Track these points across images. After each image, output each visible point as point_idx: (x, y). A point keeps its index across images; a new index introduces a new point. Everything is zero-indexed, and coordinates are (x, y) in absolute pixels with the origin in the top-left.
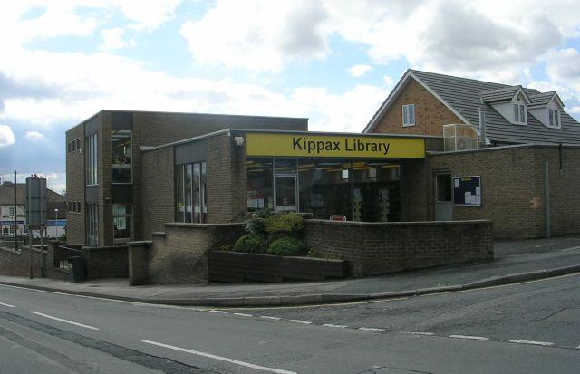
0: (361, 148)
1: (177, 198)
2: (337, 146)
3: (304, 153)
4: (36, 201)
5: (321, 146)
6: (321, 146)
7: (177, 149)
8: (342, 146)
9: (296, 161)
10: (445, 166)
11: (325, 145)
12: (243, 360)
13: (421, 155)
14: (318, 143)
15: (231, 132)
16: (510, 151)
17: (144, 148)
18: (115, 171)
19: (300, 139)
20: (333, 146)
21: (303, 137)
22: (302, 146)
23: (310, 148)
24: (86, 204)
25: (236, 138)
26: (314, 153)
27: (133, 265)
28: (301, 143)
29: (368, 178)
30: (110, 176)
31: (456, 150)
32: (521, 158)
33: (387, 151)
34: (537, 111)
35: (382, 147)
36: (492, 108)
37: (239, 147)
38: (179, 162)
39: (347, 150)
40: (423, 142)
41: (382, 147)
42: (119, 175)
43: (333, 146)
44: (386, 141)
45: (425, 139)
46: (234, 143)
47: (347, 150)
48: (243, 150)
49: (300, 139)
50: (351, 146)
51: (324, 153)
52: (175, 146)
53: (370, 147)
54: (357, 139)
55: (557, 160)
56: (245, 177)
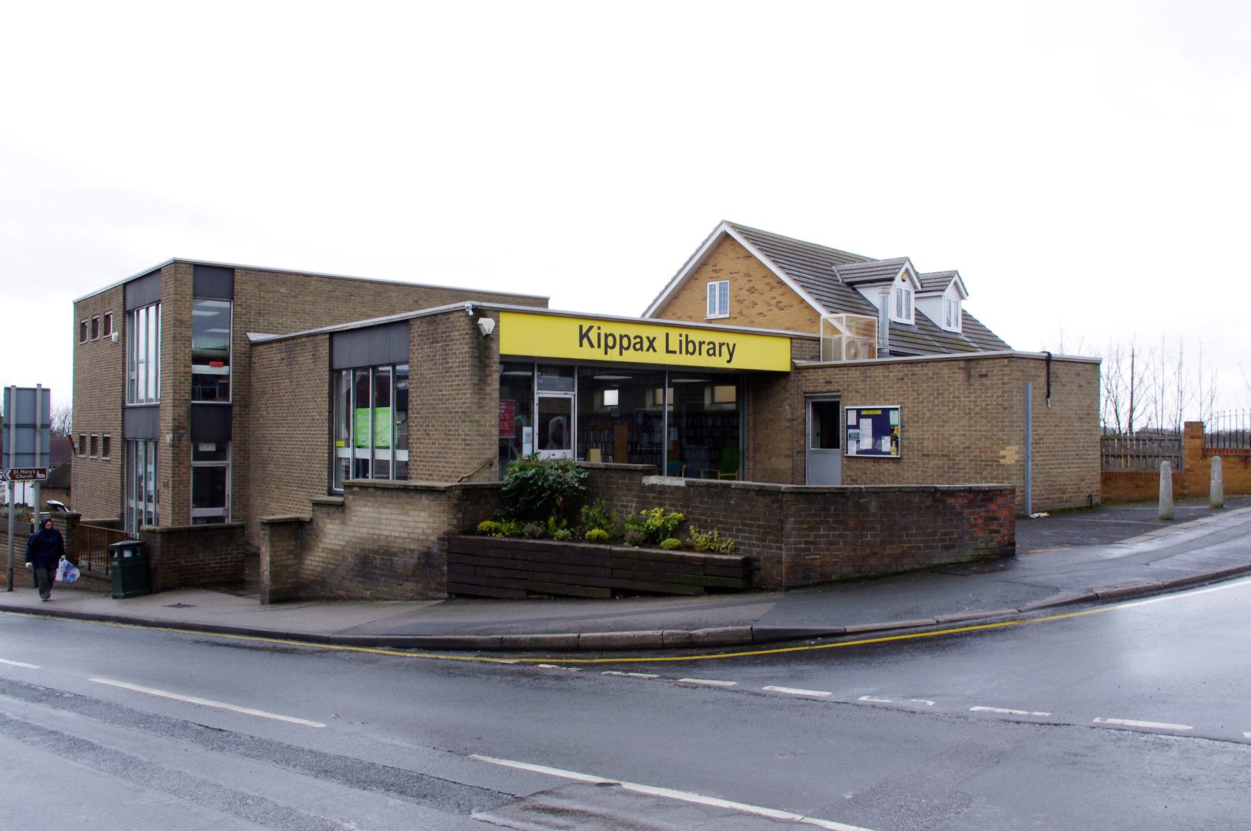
0: (691, 349)
1: (333, 436)
2: (651, 342)
3: (597, 354)
4: (26, 433)
5: (625, 342)
6: (625, 342)
7: (338, 342)
8: (660, 344)
9: (533, 365)
10: (828, 387)
11: (633, 342)
12: (793, 651)
13: (783, 365)
14: (621, 337)
15: (475, 309)
16: (962, 364)
17: (254, 337)
18: (197, 378)
19: (591, 328)
20: (646, 344)
21: (596, 324)
22: (595, 343)
23: (606, 345)
24: (124, 439)
25: (482, 321)
26: (614, 356)
27: (272, 563)
28: (593, 335)
29: (713, 402)
30: (187, 387)
31: (844, 360)
32: (982, 376)
33: (731, 355)
34: (865, 289)
35: (724, 348)
36: (858, 293)
37: (488, 335)
38: (336, 366)
39: (668, 351)
40: (787, 343)
41: (724, 348)
42: (204, 386)
43: (646, 344)
44: (730, 339)
45: (792, 338)
46: (477, 329)
47: (668, 351)
48: (493, 345)
49: (591, 328)
50: (674, 346)
51: (631, 356)
52: (332, 334)
53: (705, 348)
54: (684, 332)
55: (1043, 380)
56: (496, 385)
